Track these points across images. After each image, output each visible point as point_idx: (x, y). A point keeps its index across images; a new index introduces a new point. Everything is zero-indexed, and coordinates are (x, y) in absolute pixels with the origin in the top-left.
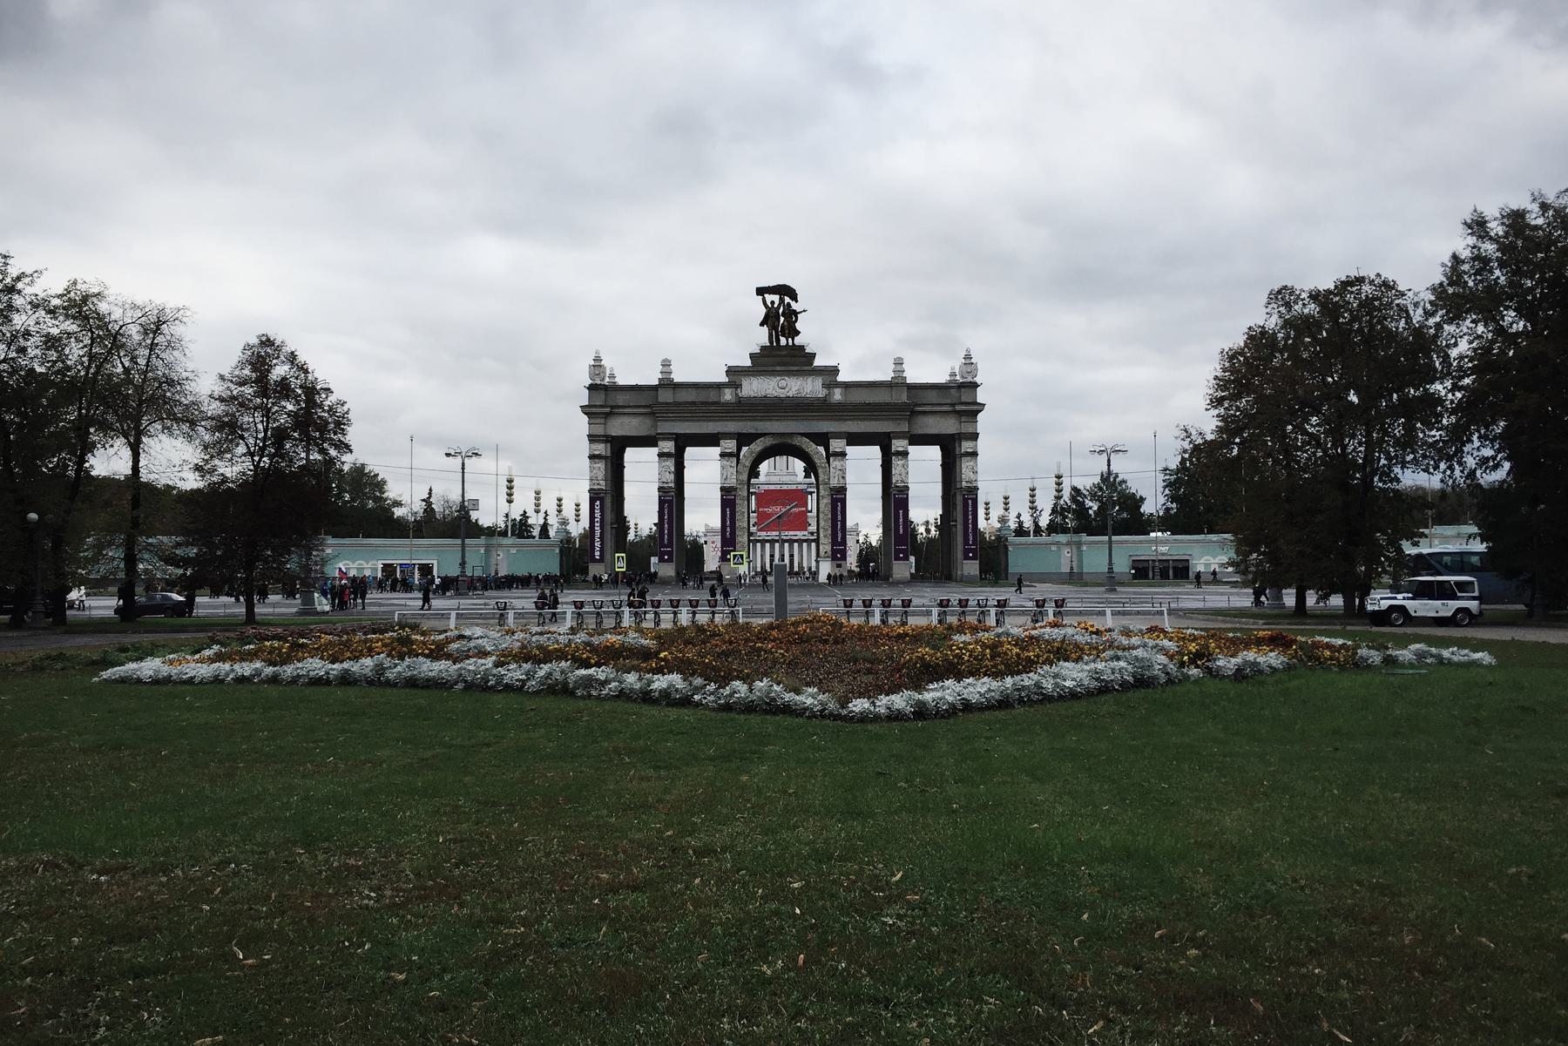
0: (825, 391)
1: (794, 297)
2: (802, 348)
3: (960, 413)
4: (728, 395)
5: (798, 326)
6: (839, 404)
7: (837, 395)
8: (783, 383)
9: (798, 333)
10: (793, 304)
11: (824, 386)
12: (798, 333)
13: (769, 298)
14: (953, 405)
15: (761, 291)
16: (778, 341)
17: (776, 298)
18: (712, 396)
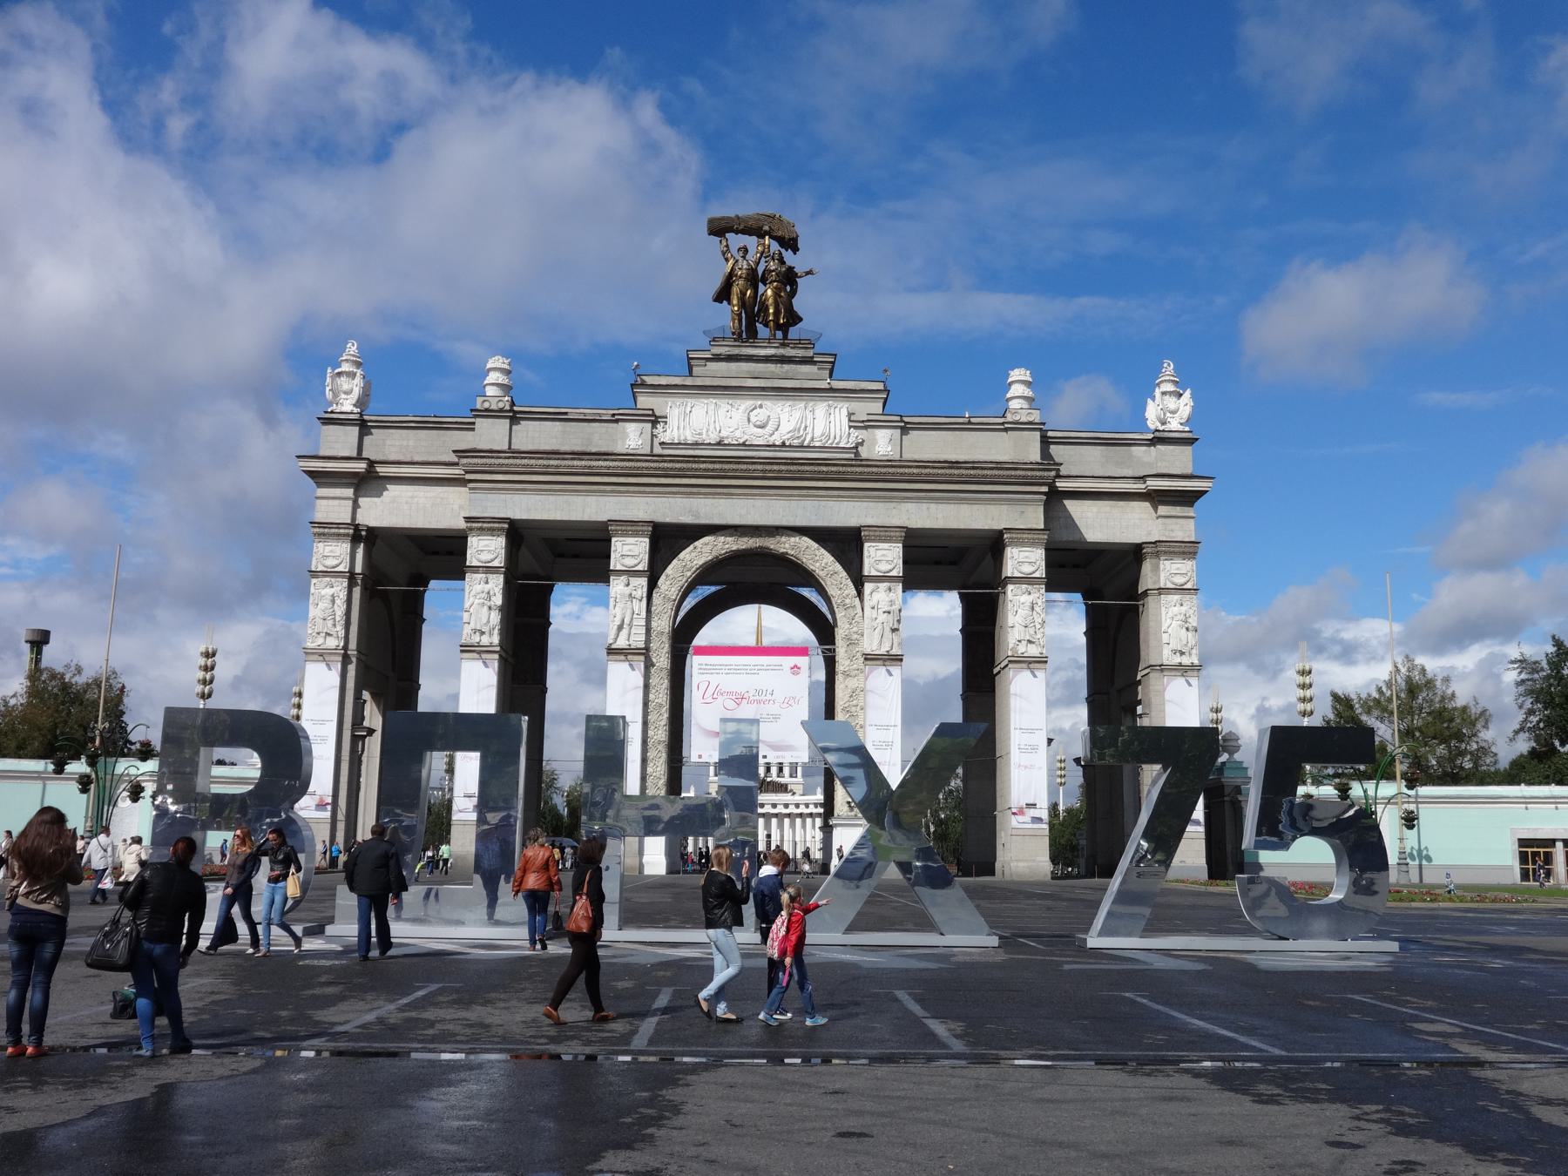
0: (857, 435)
1: (791, 244)
2: (810, 344)
3: (1157, 498)
4: (633, 438)
5: (798, 304)
6: (889, 463)
7: (882, 444)
8: (759, 416)
9: (794, 319)
10: (788, 255)
11: (855, 424)
13: (736, 240)
14: (1143, 478)
15: (719, 229)
16: (752, 334)
17: (751, 241)
18: (597, 437)
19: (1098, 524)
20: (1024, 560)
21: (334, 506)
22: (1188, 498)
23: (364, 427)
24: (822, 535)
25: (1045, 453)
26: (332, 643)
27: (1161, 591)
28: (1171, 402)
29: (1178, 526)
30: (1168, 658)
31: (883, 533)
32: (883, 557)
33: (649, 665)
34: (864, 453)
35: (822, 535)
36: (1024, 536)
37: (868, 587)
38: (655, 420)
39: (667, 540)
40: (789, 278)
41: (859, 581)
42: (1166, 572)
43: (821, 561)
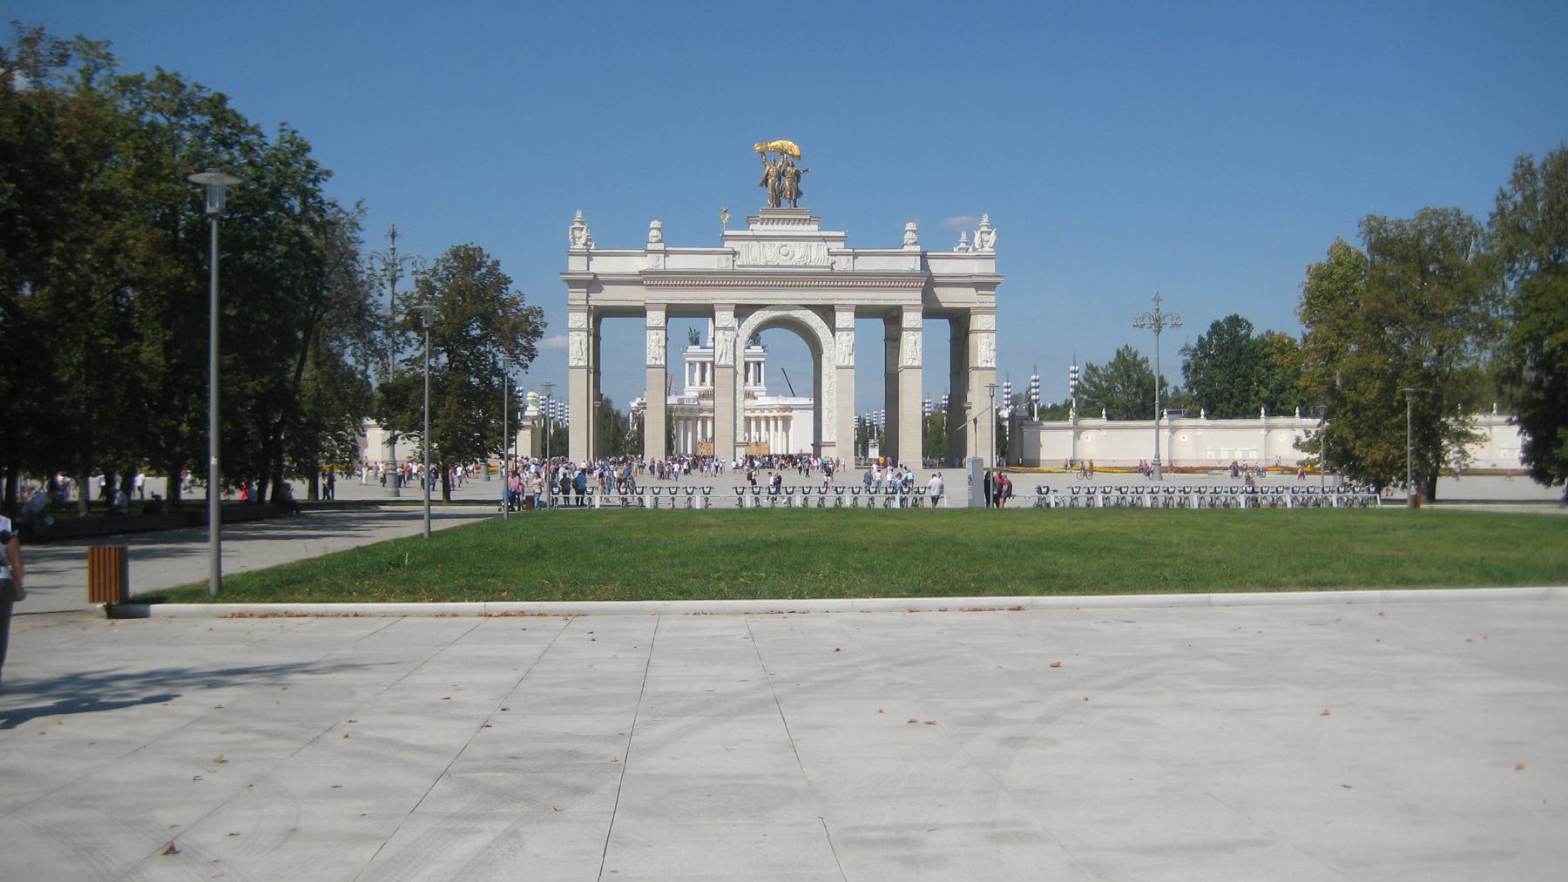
3: (979, 286)
7: (843, 264)
11: (831, 254)
12: (799, 194)
19: (949, 298)
20: (911, 319)
21: (578, 296)
22: (991, 286)
23: (590, 256)
24: (816, 308)
25: (924, 265)
26: (582, 363)
27: (977, 331)
28: (985, 237)
29: (989, 299)
30: (981, 364)
31: (845, 308)
32: (844, 319)
33: (735, 373)
34: (836, 268)
35: (816, 308)
36: (912, 308)
37: (838, 334)
38: (734, 254)
39: (742, 311)
40: (797, 175)
41: (833, 330)
42: (977, 322)
43: (814, 321)
